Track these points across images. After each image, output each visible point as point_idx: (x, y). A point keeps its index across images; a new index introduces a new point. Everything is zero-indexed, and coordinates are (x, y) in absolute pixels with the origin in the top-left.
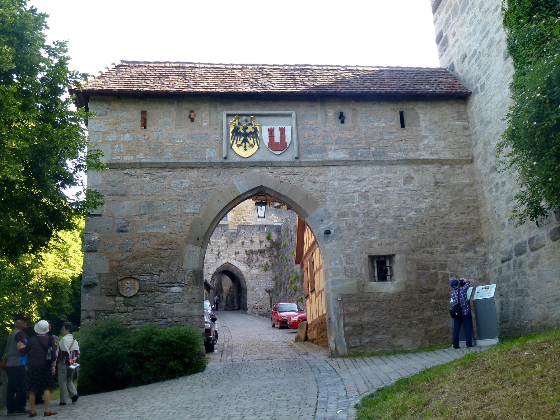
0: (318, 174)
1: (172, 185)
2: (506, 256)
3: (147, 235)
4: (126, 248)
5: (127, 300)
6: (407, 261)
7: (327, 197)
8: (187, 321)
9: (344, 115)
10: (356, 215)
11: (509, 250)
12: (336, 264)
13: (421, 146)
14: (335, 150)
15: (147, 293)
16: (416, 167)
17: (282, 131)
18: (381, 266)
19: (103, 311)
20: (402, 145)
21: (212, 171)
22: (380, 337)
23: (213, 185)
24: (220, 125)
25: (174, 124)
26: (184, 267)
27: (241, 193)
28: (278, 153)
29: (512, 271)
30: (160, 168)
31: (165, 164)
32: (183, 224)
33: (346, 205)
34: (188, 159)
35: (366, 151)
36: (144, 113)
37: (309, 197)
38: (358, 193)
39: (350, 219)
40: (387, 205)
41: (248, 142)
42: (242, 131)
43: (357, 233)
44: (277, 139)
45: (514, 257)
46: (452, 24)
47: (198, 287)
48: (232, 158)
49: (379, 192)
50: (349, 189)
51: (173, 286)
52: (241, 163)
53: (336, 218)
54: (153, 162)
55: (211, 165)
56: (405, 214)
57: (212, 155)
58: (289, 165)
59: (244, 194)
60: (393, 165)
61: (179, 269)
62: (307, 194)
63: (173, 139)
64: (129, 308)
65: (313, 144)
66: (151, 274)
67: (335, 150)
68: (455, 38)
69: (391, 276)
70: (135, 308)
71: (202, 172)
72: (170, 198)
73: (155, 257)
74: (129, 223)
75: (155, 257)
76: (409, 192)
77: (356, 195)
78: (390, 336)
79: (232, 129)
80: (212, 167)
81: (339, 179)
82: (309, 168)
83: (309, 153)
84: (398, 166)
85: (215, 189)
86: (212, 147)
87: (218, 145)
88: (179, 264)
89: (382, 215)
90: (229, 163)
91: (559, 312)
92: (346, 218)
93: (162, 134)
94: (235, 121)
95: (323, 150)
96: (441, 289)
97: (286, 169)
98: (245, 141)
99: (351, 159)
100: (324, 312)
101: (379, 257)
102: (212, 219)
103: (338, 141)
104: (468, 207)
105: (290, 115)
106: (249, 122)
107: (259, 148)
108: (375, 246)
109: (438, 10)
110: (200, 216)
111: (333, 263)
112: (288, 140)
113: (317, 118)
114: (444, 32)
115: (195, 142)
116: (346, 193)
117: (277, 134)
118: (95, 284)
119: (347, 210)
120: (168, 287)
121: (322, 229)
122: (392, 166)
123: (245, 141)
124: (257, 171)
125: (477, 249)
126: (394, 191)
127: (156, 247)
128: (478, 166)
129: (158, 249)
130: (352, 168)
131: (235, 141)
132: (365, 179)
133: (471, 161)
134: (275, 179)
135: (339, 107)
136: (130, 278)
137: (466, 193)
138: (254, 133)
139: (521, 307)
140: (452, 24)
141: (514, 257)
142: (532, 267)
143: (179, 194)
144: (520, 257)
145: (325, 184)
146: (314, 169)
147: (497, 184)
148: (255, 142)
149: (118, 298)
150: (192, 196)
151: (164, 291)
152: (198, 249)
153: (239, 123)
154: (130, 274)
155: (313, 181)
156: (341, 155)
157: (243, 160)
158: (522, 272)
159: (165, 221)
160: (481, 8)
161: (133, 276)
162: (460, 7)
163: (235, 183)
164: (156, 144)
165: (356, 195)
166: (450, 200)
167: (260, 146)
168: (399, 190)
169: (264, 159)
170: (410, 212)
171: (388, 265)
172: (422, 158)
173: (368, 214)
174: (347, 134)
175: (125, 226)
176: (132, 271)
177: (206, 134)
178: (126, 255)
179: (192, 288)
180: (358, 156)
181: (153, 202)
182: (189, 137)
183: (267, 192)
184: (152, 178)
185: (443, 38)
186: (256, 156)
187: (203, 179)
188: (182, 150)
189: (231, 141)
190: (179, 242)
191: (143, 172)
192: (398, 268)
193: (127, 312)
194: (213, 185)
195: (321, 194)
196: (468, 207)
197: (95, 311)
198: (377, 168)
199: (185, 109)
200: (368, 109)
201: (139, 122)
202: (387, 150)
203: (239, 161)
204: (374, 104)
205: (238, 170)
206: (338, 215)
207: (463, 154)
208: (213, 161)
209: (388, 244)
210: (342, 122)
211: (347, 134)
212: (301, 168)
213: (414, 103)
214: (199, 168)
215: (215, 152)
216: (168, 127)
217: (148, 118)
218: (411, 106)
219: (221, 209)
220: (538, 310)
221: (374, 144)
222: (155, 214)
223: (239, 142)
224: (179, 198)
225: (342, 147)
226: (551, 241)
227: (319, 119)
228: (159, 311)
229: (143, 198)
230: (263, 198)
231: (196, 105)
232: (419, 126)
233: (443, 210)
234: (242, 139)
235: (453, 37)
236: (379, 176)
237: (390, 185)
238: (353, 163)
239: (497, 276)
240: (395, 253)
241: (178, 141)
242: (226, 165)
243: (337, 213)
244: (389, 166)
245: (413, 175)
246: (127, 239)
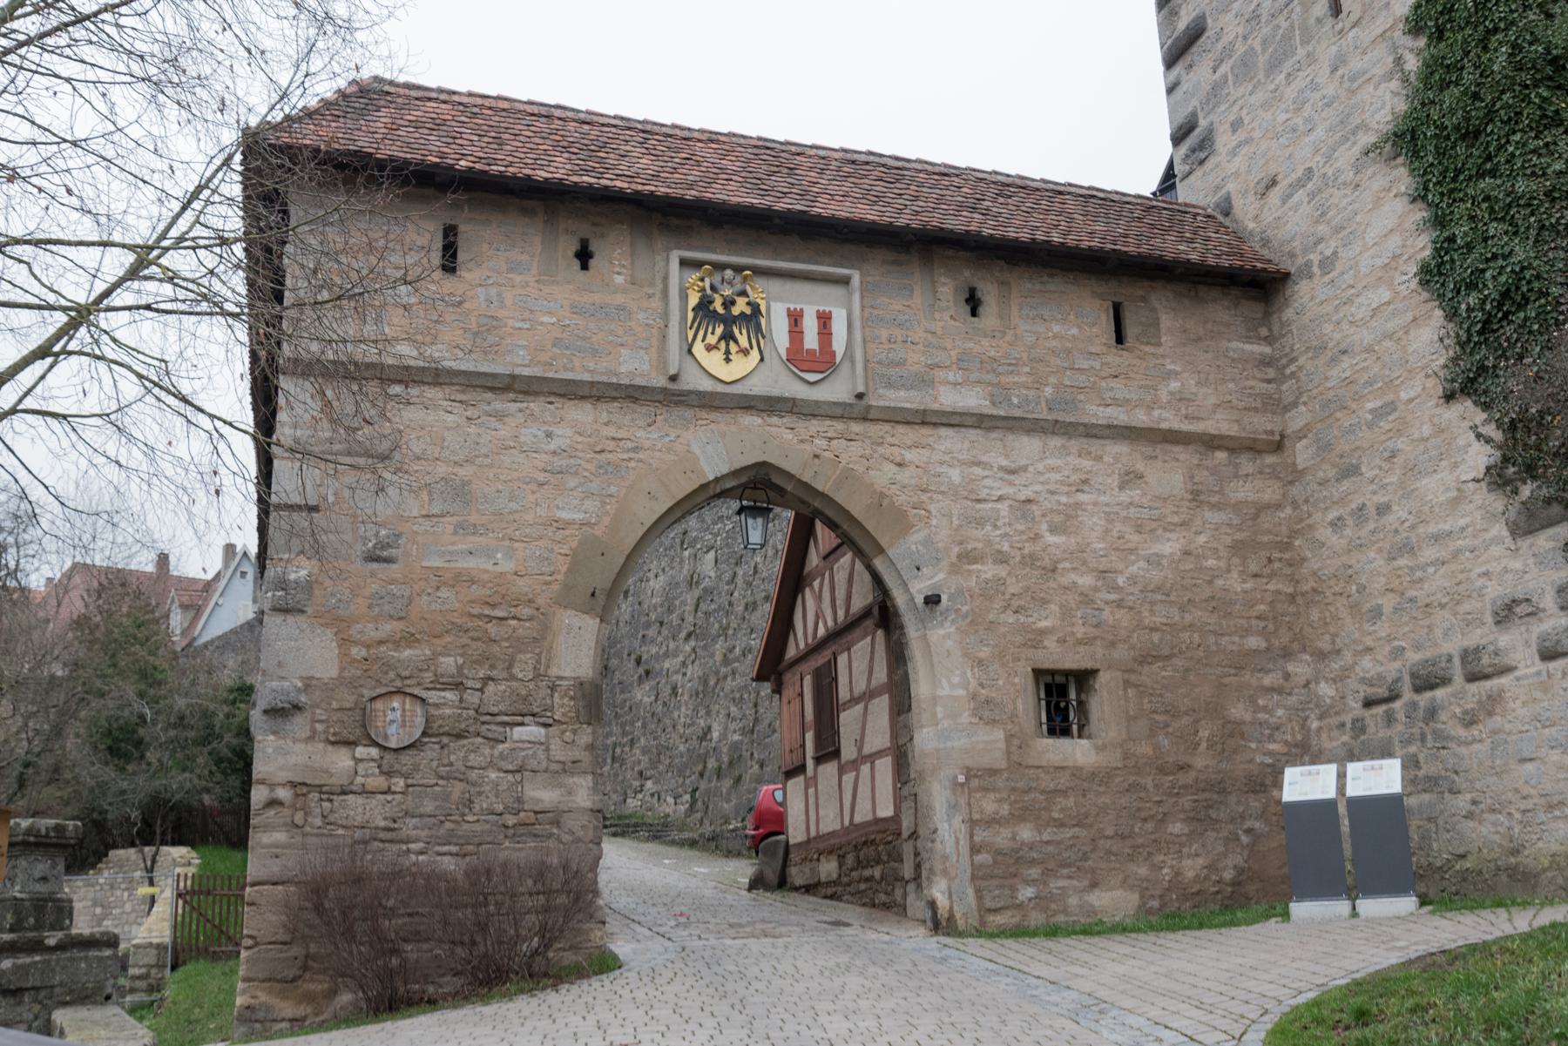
0: (909, 443)
1: (522, 439)
2: (1382, 692)
3: (448, 575)
4: (387, 608)
5: (388, 757)
6: (1125, 690)
7: (932, 508)
8: (557, 823)
9: (979, 294)
10: (1001, 558)
11: (1394, 675)
12: (952, 686)
13: (1164, 396)
14: (955, 384)
15: (445, 740)
16: (1148, 450)
17: (824, 320)
18: (1062, 698)
19: (319, 788)
20: (1119, 389)
21: (634, 411)
22: (1061, 883)
23: (636, 449)
24: (660, 286)
25: (534, 271)
26: (554, 671)
27: (711, 478)
28: (812, 377)
29: (1400, 727)
30: (492, 389)
31: (507, 380)
32: (552, 551)
33: (979, 533)
34: (572, 370)
35: (1031, 393)
36: (450, 232)
37: (886, 503)
38: (1007, 503)
39: (989, 570)
40: (1079, 539)
41: (736, 342)
42: (721, 310)
43: (1006, 608)
44: (811, 341)
45: (1408, 695)
46: (1231, 98)
47: (589, 730)
48: (694, 381)
49: (1059, 503)
50: (986, 491)
51: (522, 724)
52: (713, 395)
53: (952, 565)
54: (472, 369)
55: (632, 394)
56: (1121, 566)
57: (636, 365)
58: (839, 411)
59: (717, 480)
60: (1095, 436)
61: (538, 676)
62: (882, 495)
63: (532, 311)
64: (394, 780)
65: (901, 363)
66: (458, 686)
67: (955, 384)
68: (1241, 135)
69: (1081, 728)
70: (410, 781)
71: (605, 411)
73: (473, 639)
74: (398, 536)
75: (473, 639)
76: (1132, 510)
77: (1003, 508)
78: (1086, 883)
79: (694, 300)
80: (635, 400)
81: (963, 463)
82: (887, 427)
83: (890, 385)
84: (1107, 442)
85: (640, 461)
86: (639, 343)
87: (655, 342)
88: (538, 662)
89: (1067, 565)
90: (682, 393)
91: (1557, 836)
92: (979, 567)
93: (499, 295)
94: (702, 280)
95: (923, 382)
96: (1207, 767)
97: (828, 422)
98: (728, 337)
99: (995, 412)
100: (886, 811)
101: (1053, 673)
102: (631, 542)
103: (962, 362)
104: (1270, 560)
105: (845, 281)
106: (738, 287)
107: (762, 360)
108: (1050, 643)
109: (1187, 59)
110: (598, 531)
111: (944, 683)
112: (839, 344)
113: (911, 296)
114: (1201, 115)
115: (592, 325)
116: (979, 501)
117: (810, 326)
118: (297, 708)
119: (980, 545)
120: (505, 724)
121: (919, 591)
122: (1094, 441)
123: (728, 337)
124: (751, 420)
125: (1290, 668)
126: (1095, 504)
127: (476, 611)
128: (1299, 461)
129: (479, 616)
130: (995, 435)
131: (701, 333)
132: (1025, 469)
133: (1278, 446)
134: (802, 446)
135: (967, 273)
136: (399, 692)
137: (1266, 526)
138: (753, 318)
139: (1429, 820)
140: (1231, 98)
141: (1408, 695)
142: (1469, 721)
143: (541, 465)
144: (1428, 695)
145: (926, 472)
146: (901, 429)
147: (1362, 508)
149: (361, 751)
150: (576, 473)
151: (496, 735)
152: (591, 622)
153: (713, 288)
154: (398, 683)
155: (898, 460)
156: (972, 400)
157: (720, 388)
158: (1434, 732)
159: (503, 538)
160: (1334, 70)
161: (408, 690)
162: (1262, 60)
163: (696, 449)
164: (483, 321)
165: (1003, 508)
166: (1228, 540)
168: (1107, 505)
169: (775, 392)
170: (1133, 563)
171: (1073, 695)
172: (1164, 425)
173: (1030, 560)
174: (985, 347)
175: (389, 546)
176: (406, 673)
177: (621, 308)
178: (388, 628)
179: (574, 732)
180: (1011, 404)
181: (469, 483)
182: (576, 310)
183: (777, 480)
184: (469, 414)
185: (1197, 131)
186: (753, 380)
187: (610, 431)
188: (554, 345)
189: (691, 334)
190: (541, 601)
191: (440, 395)
192: (1104, 704)
193: (388, 791)
194: (636, 449)
195: (915, 499)
196: (1270, 560)
197: (294, 785)
198: (1055, 442)
199: (567, 231)
200: (1038, 286)
201: (436, 258)
202: (1081, 397)
203: (710, 389)
204: (1051, 276)
205: (704, 414)
206: (959, 557)
207: (1261, 424)
208: (639, 381)
209: (1080, 642)
210: (974, 313)
211: (985, 347)
212: (867, 424)
213: (1146, 283)
214: (599, 399)
215: (646, 357)
216: (518, 279)
217: (461, 244)
218: (1140, 292)
219: (656, 517)
220: (1485, 830)
221: (1052, 380)
222: (474, 518)
223: (712, 339)
224: (541, 477)
225: (974, 377)
226: (1537, 657)
227: (917, 299)
228: (480, 793)
229: (442, 469)
230: (761, 494)
231: (594, 224)
232: (1159, 345)
233: (1211, 562)
234: (719, 330)
235: (1234, 131)
236: (1059, 462)
237: (1086, 488)
238: (999, 424)
239: (1345, 738)
240: (1098, 666)
241: (546, 319)
242: (672, 397)
243: (956, 550)
244: (1085, 440)
245: (1140, 467)
246: (393, 581)
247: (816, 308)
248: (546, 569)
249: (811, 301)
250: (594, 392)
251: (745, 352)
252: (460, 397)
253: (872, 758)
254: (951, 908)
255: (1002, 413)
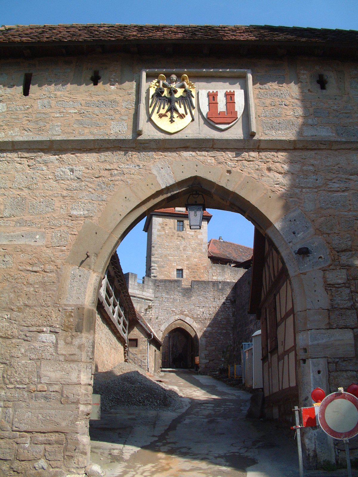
17: (230, 96)
27: (163, 187)
34: (83, 135)
41: (177, 111)
44: (222, 106)
54: (31, 139)
71: (103, 156)
72: (51, 193)
79: (152, 91)
99: (339, 139)
107: (193, 120)
123: (172, 109)
131: (157, 109)
135: (317, 68)
138: (187, 98)
148: (188, 111)
157: (168, 137)
159: (40, 228)
163: (154, 172)
167: (195, 117)
190: (59, 262)
222: (27, 217)
223: (162, 111)
224: (65, 193)
234: (166, 107)
247: (225, 91)
248: (62, 243)
249: (221, 89)
250: (97, 146)
251: (182, 116)
252: (26, 155)
253: (287, 352)
254: (315, 448)
255: (344, 140)
